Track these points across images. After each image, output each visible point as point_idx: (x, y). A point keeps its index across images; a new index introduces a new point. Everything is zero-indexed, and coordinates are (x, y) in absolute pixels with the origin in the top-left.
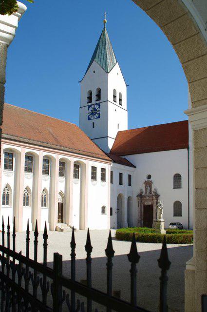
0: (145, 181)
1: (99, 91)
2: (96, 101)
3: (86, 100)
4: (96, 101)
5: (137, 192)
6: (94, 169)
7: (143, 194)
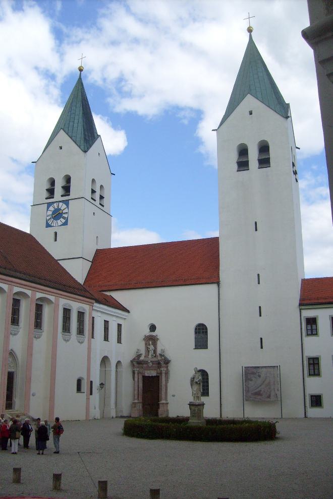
0: (145, 336)
1: (68, 179)
2: (62, 196)
3: (46, 194)
4: (62, 196)
5: (131, 355)
6: (67, 312)
7: (142, 358)
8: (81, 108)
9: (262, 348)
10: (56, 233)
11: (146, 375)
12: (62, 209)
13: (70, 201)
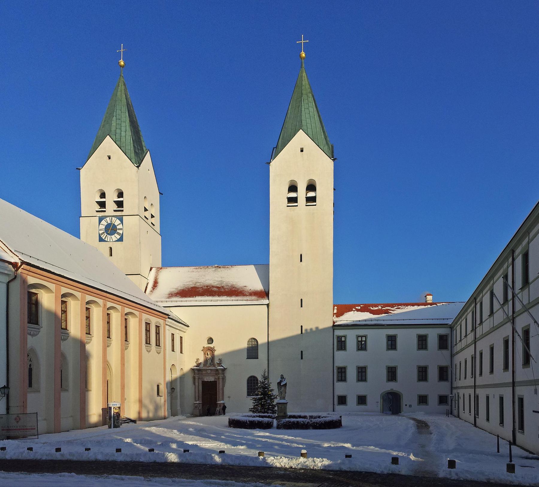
9: (302, 358)
10: (111, 248)
11: (205, 380)
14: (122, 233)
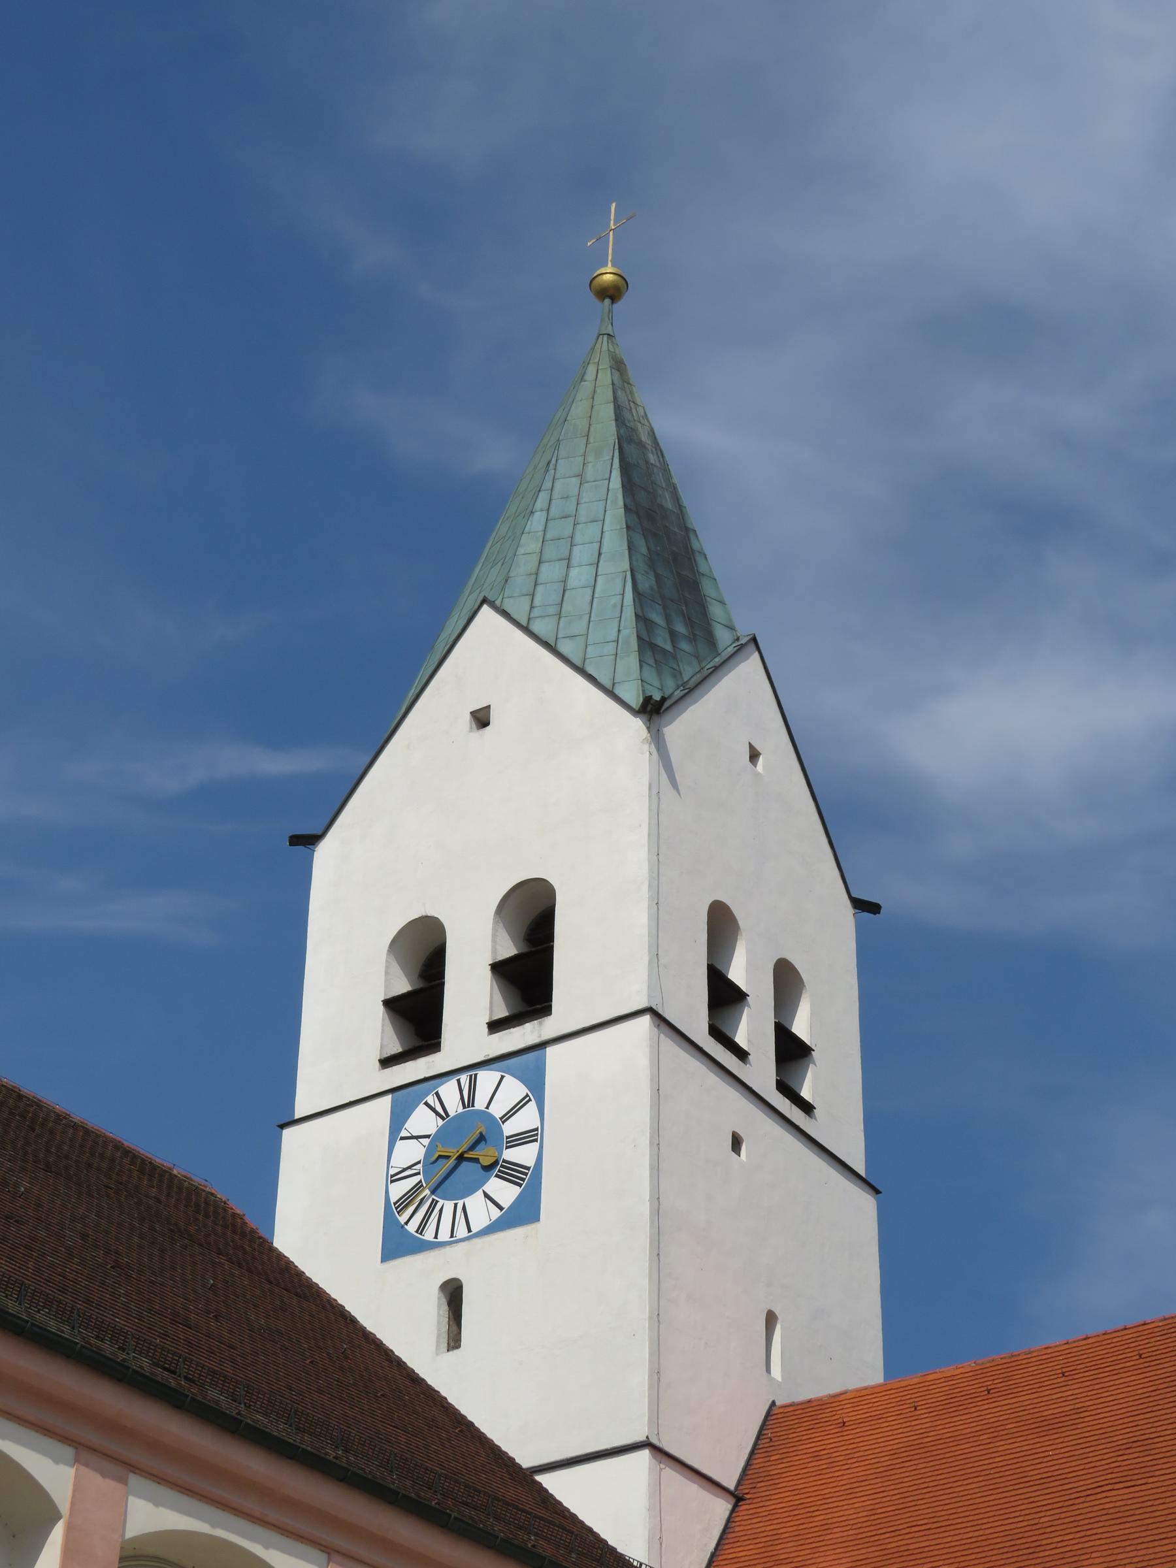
2: (495, 1026)
8: (616, 482)
12: (497, 1111)
13: (550, 1051)
14: (530, 1163)
